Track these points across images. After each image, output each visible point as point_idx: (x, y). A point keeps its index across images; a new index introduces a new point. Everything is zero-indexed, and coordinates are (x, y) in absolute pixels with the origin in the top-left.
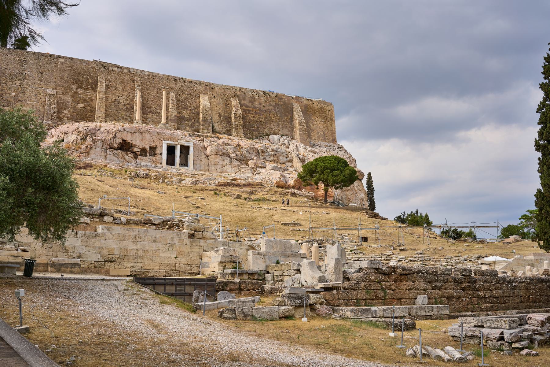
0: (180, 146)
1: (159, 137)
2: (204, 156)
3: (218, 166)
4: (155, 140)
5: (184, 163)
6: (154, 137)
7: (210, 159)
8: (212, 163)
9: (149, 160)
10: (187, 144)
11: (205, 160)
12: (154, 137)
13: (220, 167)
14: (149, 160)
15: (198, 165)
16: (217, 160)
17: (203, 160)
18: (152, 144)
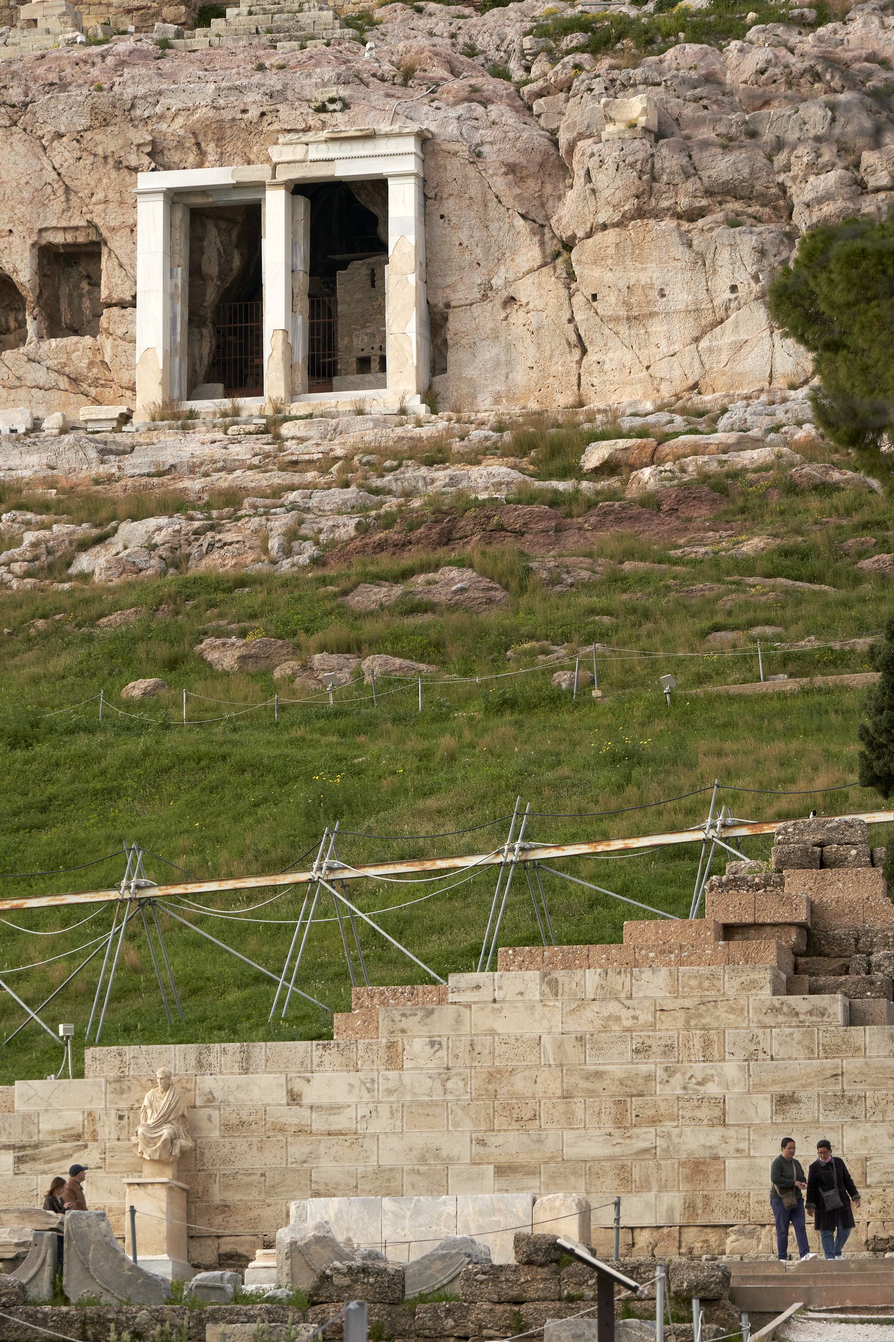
0: (299, 189)
1: (106, 141)
2: (529, 253)
3: (657, 327)
4: (83, 178)
5: (335, 354)
6: (62, 153)
7: (590, 274)
8: (609, 304)
9: (38, 374)
10: (351, 164)
11: (539, 292)
12: (62, 153)
13: (684, 329)
14: (38, 374)
15: (488, 353)
16: (650, 274)
17: (525, 291)
18: (60, 223)
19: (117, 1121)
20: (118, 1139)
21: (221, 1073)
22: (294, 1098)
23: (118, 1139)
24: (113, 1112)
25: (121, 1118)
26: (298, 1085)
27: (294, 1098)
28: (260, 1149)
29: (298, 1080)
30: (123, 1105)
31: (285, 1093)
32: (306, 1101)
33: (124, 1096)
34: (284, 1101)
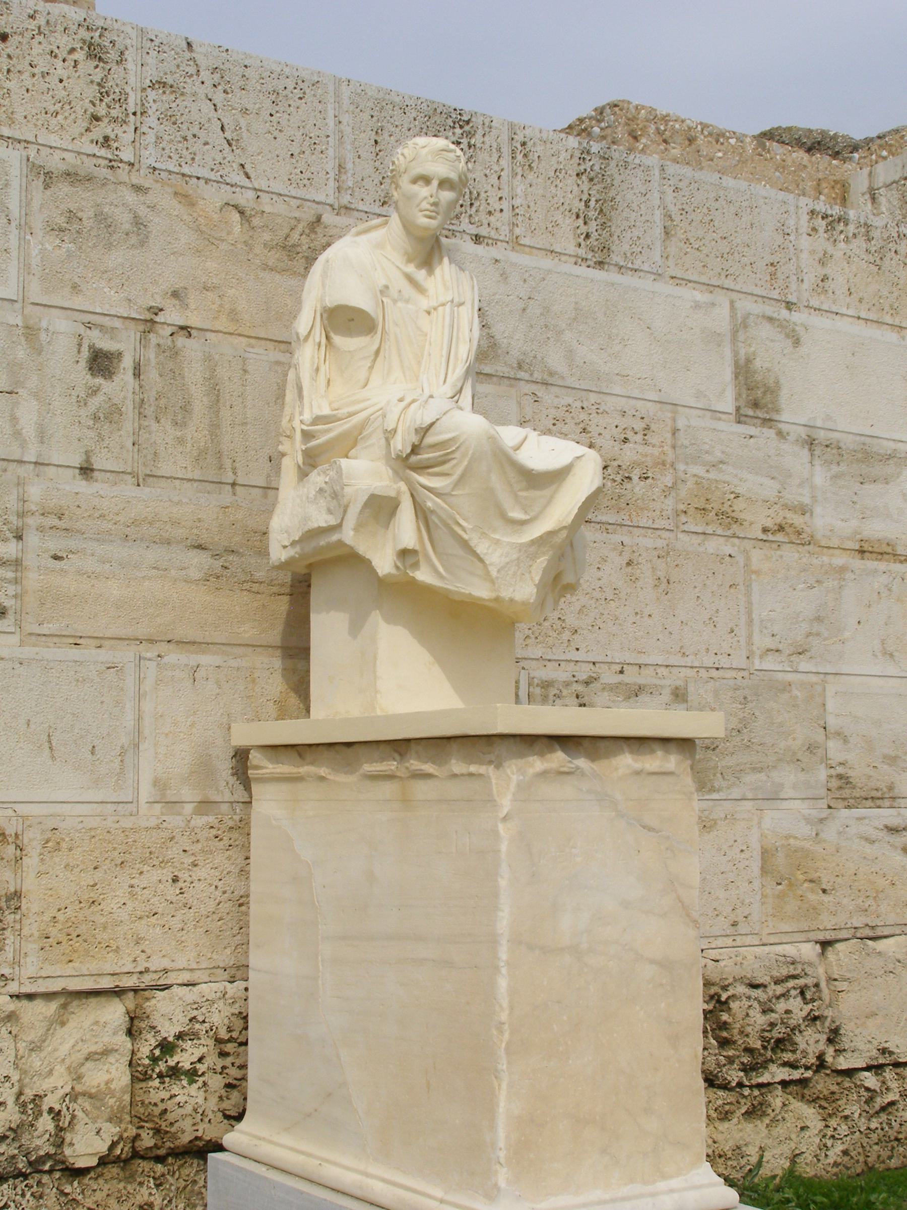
19: (81, 376)
20: (86, 471)
21: (515, 243)
22: (757, 401)
23: (86, 471)
24: (62, 324)
25: (101, 363)
26: (768, 351)
27: (757, 401)
28: (664, 584)
29: (765, 331)
30: (107, 299)
31: (728, 374)
32: (795, 413)
33: (116, 258)
34: (728, 404)
